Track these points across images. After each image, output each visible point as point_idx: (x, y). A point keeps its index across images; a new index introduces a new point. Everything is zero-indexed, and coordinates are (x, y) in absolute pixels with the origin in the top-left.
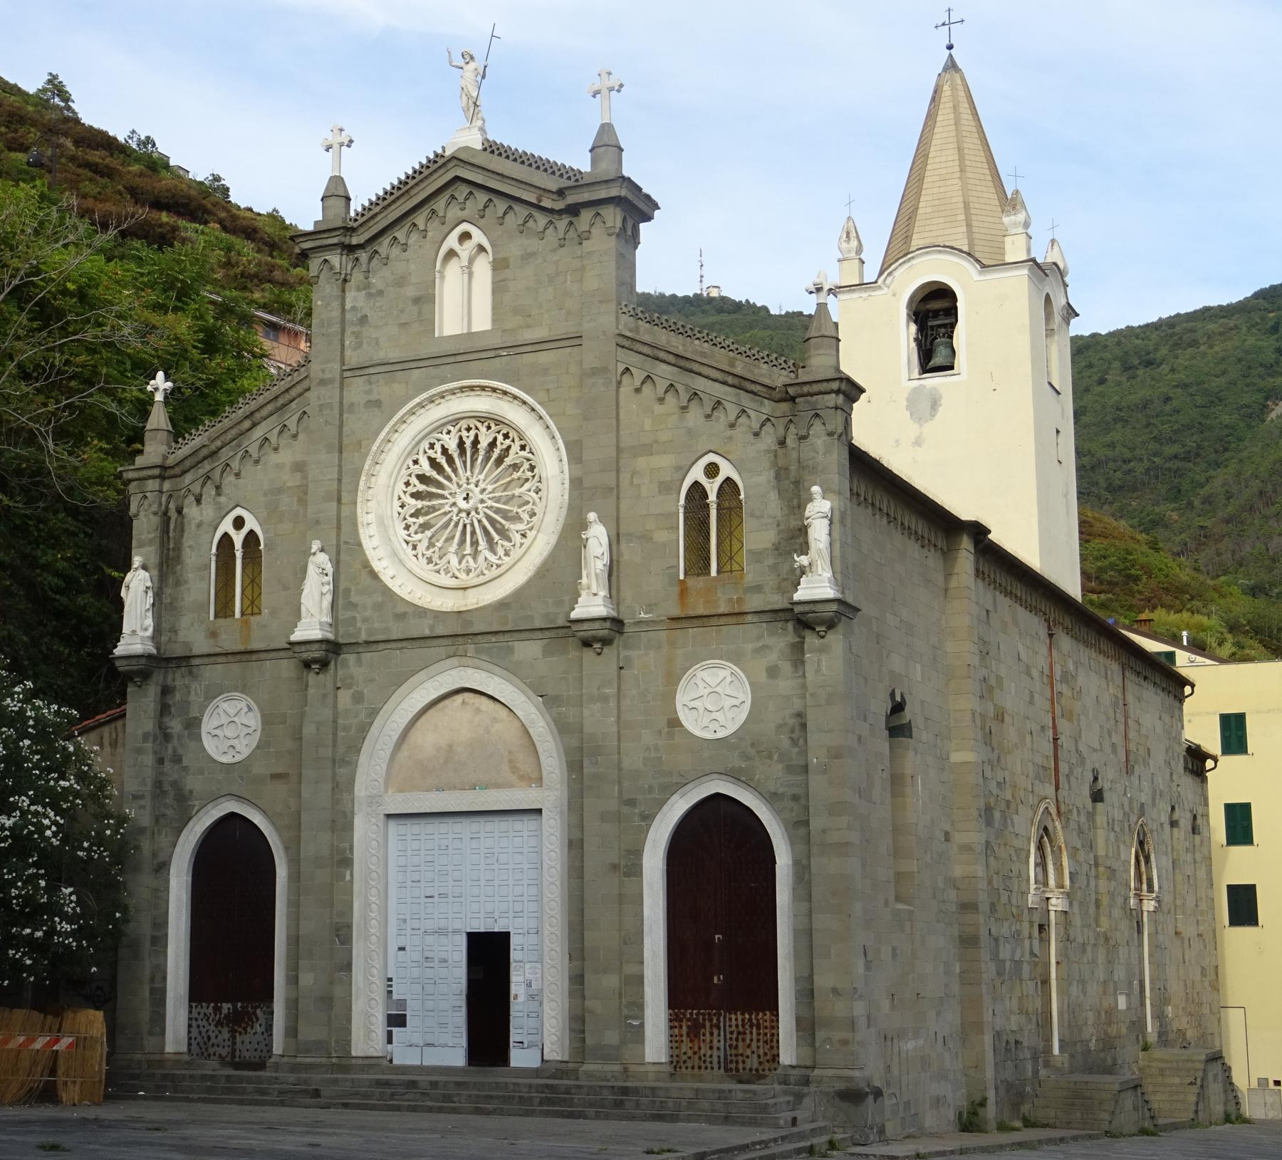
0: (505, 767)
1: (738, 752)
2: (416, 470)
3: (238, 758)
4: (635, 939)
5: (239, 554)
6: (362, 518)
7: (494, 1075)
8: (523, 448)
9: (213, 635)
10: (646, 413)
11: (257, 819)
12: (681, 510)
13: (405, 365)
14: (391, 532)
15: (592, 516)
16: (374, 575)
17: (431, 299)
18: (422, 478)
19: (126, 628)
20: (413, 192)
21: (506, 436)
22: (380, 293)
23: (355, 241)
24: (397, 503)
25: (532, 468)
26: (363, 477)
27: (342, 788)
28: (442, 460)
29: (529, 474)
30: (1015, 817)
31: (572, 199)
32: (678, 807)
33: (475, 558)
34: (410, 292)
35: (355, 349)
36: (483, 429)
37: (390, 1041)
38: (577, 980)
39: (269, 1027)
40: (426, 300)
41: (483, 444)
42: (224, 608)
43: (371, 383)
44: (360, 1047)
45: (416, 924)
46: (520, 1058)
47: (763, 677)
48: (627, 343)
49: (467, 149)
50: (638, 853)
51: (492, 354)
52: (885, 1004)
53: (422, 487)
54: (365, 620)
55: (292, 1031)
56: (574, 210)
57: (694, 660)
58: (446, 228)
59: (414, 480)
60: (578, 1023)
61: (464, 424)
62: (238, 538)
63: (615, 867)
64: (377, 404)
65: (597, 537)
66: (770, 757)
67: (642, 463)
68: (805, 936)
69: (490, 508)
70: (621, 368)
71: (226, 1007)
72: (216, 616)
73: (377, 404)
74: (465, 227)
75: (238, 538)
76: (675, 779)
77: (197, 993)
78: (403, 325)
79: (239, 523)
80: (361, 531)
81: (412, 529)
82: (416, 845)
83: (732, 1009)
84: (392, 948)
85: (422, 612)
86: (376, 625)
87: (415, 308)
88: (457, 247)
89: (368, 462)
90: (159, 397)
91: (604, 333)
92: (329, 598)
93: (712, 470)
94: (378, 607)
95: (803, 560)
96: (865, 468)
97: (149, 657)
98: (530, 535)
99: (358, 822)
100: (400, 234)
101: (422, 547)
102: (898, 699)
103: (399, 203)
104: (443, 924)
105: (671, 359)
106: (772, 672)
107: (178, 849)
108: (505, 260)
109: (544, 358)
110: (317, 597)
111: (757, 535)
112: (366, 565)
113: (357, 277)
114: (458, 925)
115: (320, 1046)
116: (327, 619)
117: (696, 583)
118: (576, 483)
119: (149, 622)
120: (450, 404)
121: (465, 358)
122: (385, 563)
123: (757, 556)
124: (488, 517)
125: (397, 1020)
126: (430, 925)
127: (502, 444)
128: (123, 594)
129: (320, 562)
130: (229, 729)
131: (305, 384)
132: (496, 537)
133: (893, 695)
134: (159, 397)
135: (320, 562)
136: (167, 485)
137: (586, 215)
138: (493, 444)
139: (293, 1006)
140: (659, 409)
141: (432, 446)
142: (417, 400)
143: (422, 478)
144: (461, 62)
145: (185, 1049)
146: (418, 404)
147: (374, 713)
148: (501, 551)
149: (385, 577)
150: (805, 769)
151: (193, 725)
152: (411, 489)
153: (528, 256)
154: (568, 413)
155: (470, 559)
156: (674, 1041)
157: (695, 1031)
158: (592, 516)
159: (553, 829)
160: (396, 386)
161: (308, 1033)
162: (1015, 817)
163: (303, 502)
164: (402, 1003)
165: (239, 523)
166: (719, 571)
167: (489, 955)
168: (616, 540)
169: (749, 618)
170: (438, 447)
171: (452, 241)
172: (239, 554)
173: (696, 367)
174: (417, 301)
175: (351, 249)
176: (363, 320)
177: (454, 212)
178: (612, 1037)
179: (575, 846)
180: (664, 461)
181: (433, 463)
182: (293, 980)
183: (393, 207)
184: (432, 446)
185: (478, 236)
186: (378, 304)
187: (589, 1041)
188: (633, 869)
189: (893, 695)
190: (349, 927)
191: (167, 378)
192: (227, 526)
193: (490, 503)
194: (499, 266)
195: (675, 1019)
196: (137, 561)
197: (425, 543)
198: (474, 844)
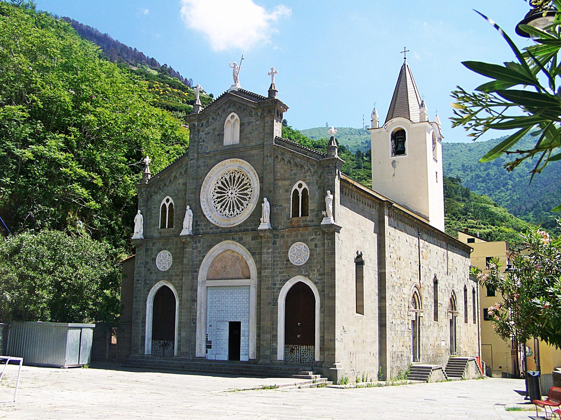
0: (240, 273)
1: (305, 270)
2: (218, 185)
3: (166, 270)
4: (275, 323)
5: (168, 210)
7: (235, 363)
8: (248, 179)
9: (160, 233)
11: (171, 287)
14: (210, 203)
15: (265, 199)
16: (204, 216)
18: (219, 188)
19: (135, 231)
21: (243, 175)
22: (209, 133)
25: (250, 185)
27: (195, 278)
28: (225, 182)
29: (249, 186)
30: (404, 289)
32: (288, 285)
34: (217, 133)
37: (207, 353)
38: (258, 336)
39: (174, 348)
40: (221, 135)
42: (163, 226)
44: (198, 354)
45: (214, 319)
46: (243, 358)
47: (313, 247)
50: (277, 299)
52: (351, 344)
53: (219, 190)
54: (202, 229)
55: (179, 349)
59: (217, 188)
60: (258, 348)
62: (167, 205)
63: (270, 303)
64: (207, 165)
65: (266, 206)
66: (314, 271)
67: (280, 183)
68: (322, 323)
71: (162, 341)
72: (161, 228)
74: (233, 114)
75: (167, 205)
76: (287, 277)
77: (155, 337)
79: (168, 200)
81: (216, 202)
82: (215, 296)
83: (302, 345)
84: (208, 326)
86: (205, 231)
88: (230, 120)
92: (191, 223)
93: (300, 186)
94: (205, 225)
95: (324, 213)
97: (142, 239)
98: (249, 204)
99: (199, 288)
101: (218, 208)
102: (359, 253)
104: (222, 319)
106: (316, 246)
107: (149, 296)
108: (244, 123)
110: (188, 222)
111: (312, 205)
114: (226, 319)
115: (187, 353)
116: (191, 229)
117: (296, 219)
118: (261, 189)
119: (142, 230)
121: (232, 152)
123: (313, 211)
124: (237, 199)
125: (209, 347)
126: (218, 319)
127: (242, 178)
128: (135, 221)
129: (189, 213)
130: (164, 260)
132: (240, 205)
133: (357, 252)
135: (189, 213)
138: (239, 178)
139: (179, 341)
141: (222, 178)
143: (219, 188)
145: (150, 353)
147: (204, 257)
148: (241, 209)
150: (324, 275)
151: (154, 260)
152: (216, 191)
153: (249, 123)
156: (286, 354)
157: (292, 350)
158: (265, 199)
159: (253, 291)
161: (183, 350)
162: (404, 289)
163: (185, 194)
164: (210, 342)
165: (168, 200)
166: (302, 216)
167: (235, 328)
168: (271, 206)
170: (224, 178)
171: (229, 117)
172: (168, 210)
174: (218, 135)
178: (268, 353)
179: (259, 296)
181: (222, 183)
182: (179, 334)
184: (222, 178)
185: (236, 116)
187: (261, 354)
188: (276, 304)
189: (357, 252)
190: (196, 320)
192: (164, 201)
193: (238, 195)
194: (242, 125)
195: (285, 348)
196: (139, 211)
197: (220, 207)
198: (231, 295)
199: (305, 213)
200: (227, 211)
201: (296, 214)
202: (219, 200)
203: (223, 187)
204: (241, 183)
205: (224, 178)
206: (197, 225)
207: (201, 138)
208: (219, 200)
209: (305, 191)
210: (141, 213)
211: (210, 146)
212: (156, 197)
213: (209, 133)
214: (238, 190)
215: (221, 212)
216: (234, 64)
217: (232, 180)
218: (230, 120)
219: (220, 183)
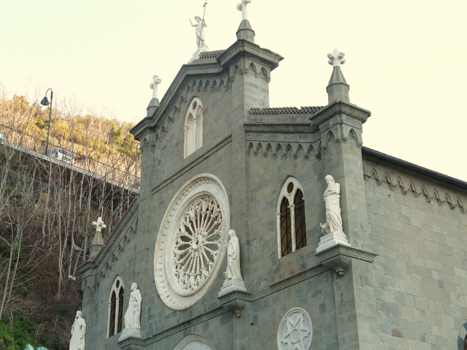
6: (157, 266)
10: (258, 164)
12: (278, 217)
13: (172, 179)
16: (158, 296)
18: (184, 238)
21: (212, 203)
23: (153, 125)
24: (173, 255)
26: (157, 244)
28: (189, 226)
33: (200, 275)
36: (203, 202)
40: (180, 143)
41: (204, 210)
48: (248, 129)
49: (195, 61)
56: (226, 69)
57: (285, 309)
58: (187, 104)
59: (180, 240)
61: (196, 203)
69: (207, 245)
70: (248, 143)
74: (195, 99)
80: (155, 273)
85: (175, 311)
89: (159, 235)
90: (99, 230)
92: (138, 314)
94: (160, 314)
95: (324, 226)
96: (371, 157)
105: (266, 129)
106: (322, 307)
109: (221, 153)
112: (156, 290)
113: (158, 144)
122: (165, 290)
134: (99, 230)
136: (95, 272)
137: (232, 69)
138: (207, 210)
140: (265, 160)
144: (195, 22)
149: (162, 297)
152: (179, 245)
155: (198, 277)
169: (309, 275)
170: (188, 219)
173: (278, 129)
174: (177, 144)
175: (153, 129)
176: (159, 162)
177: (190, 95)
180: (268, 190)
181: (187, 229)
191: (104, 220)
199: (302, 242)
200: (192, 278)
201: (286, 249)
202: (181, 261)
203: (187, 234)
204: (210, 217)
205: (188, 219)
206: (150, 317)
207: (156, 159)
208: (181, 261)
209: (299, 194)
210: (83, 317)
211: (168, 168)
212: (104, 283)
213: (165, 147)
214: (206, 234)
215: (184, 282)
216: (196, 18)
217: (199, 217)
219: (183, 229)
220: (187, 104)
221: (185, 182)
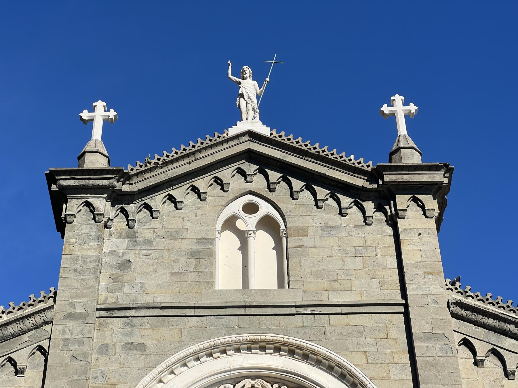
17: (211, 255)
20: (198, 156)
23: (126, 188)
31: (389, 177)
35: (112, 291)
43: (132, 326)
51: (293, 310)
64: (141, 347)
73: (141, 347)
78: (173, 274)
87: (193, 261)
91: (435, 301)
100: (177, 193)
103: (181, 162)
120: (231, 358)
131: (49, 314)
142: (195, 348)
146: (196, 353)
154: (392, 378)
160: (165, 332)
174: (194, 254)
183: (175, 165)
185: (265, 208)
186: (143, 252)
218: (242, 214)
220: (229, 195)
221: (228, 331)
